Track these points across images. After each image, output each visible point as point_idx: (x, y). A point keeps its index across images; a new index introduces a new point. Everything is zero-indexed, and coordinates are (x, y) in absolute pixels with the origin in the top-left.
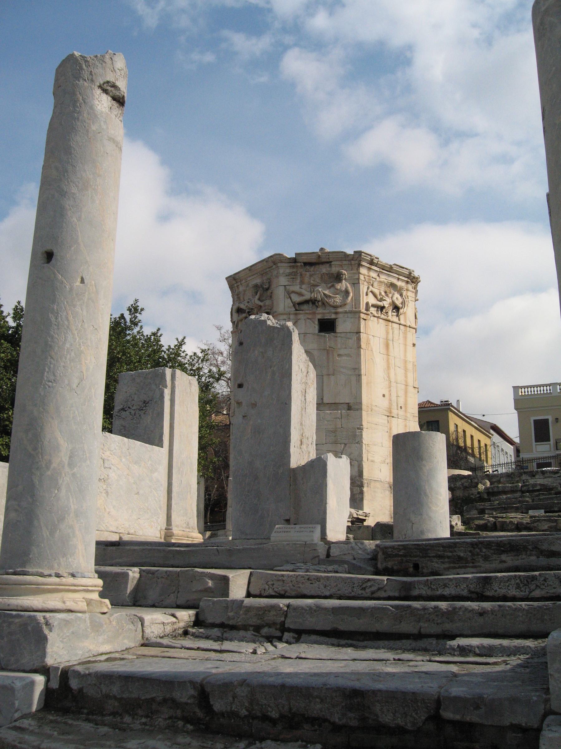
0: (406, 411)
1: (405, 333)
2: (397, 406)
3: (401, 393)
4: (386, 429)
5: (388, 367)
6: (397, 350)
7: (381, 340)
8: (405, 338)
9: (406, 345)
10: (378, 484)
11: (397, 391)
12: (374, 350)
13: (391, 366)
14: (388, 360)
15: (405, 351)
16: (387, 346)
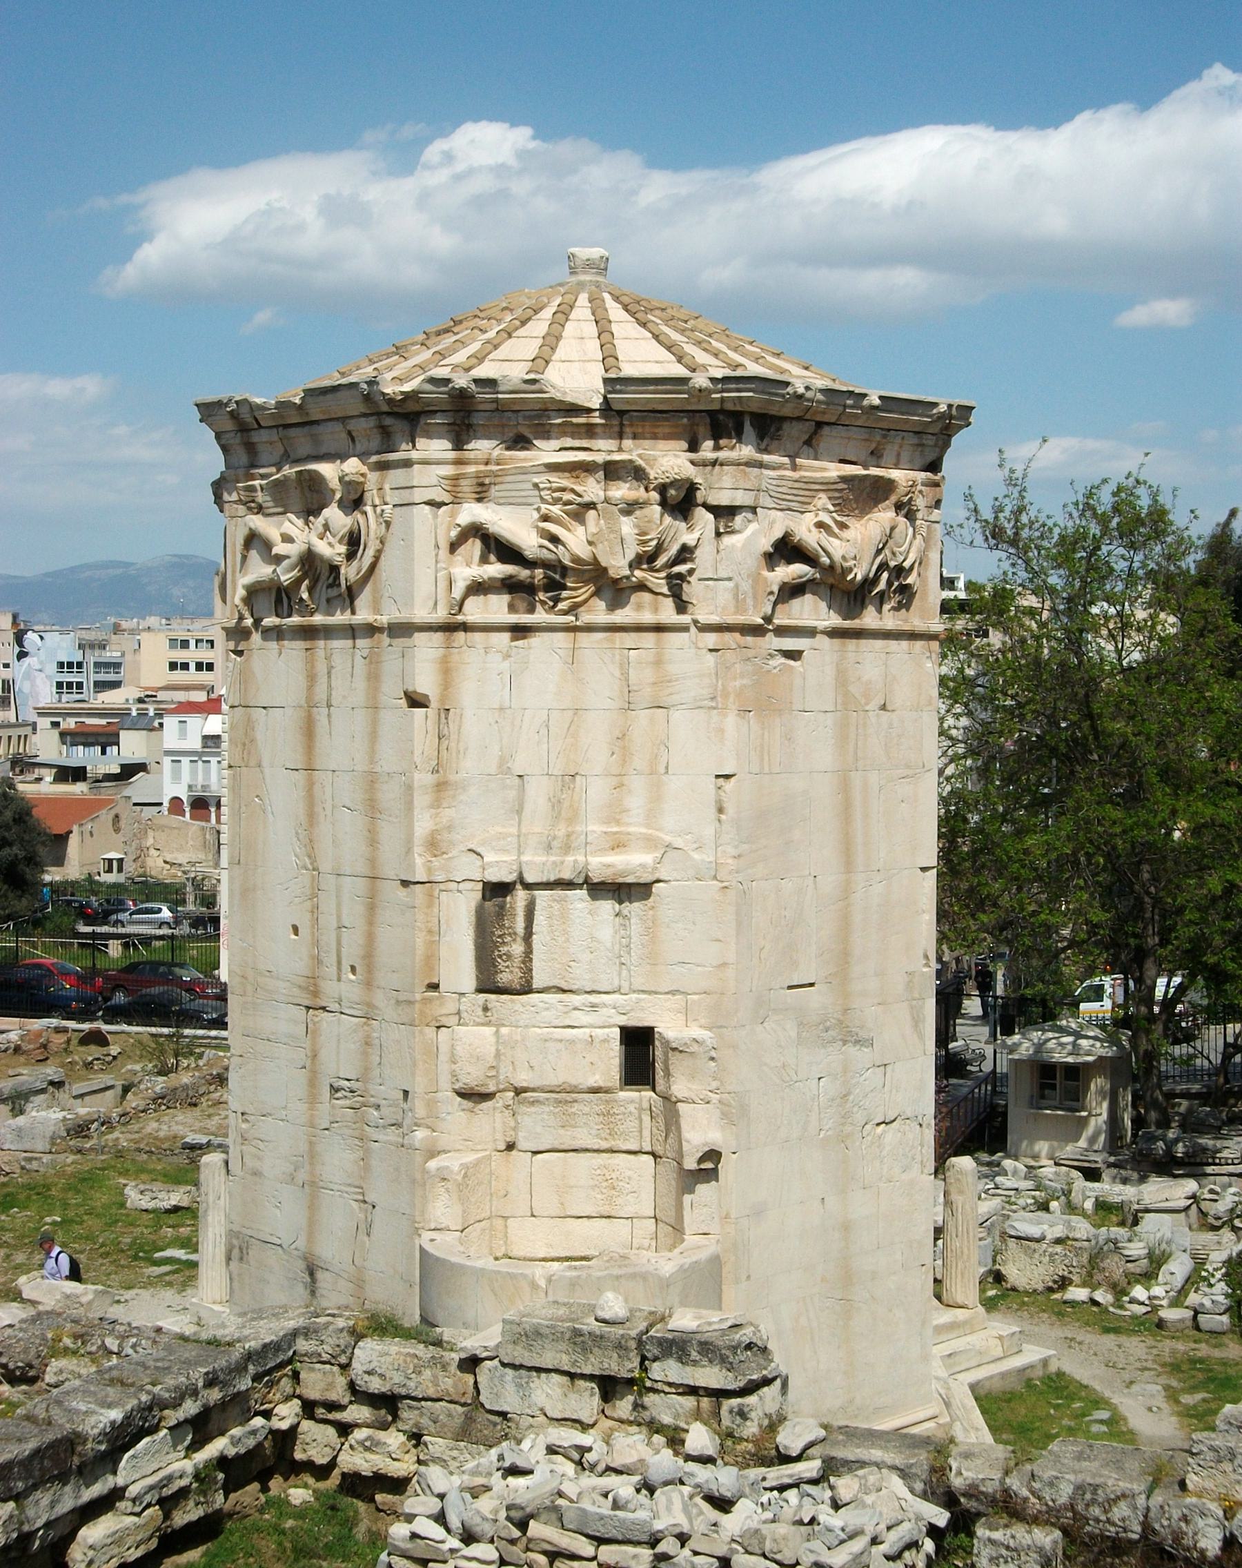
0: (368, 984)
1: (373, 660)
2: (339, 963)
3: (353, 913)
4: (301, 1056)
5: (311, 816)
6: (341, 744)
7: (289, 711)
8: (374, 677)
9: (374, 707)
10: (273, 1257)
11: (339, 905)
12: (265, 763)
13: (318, 809)
14: (310, 785)
15: (373, 736)
16: (309, 731)
